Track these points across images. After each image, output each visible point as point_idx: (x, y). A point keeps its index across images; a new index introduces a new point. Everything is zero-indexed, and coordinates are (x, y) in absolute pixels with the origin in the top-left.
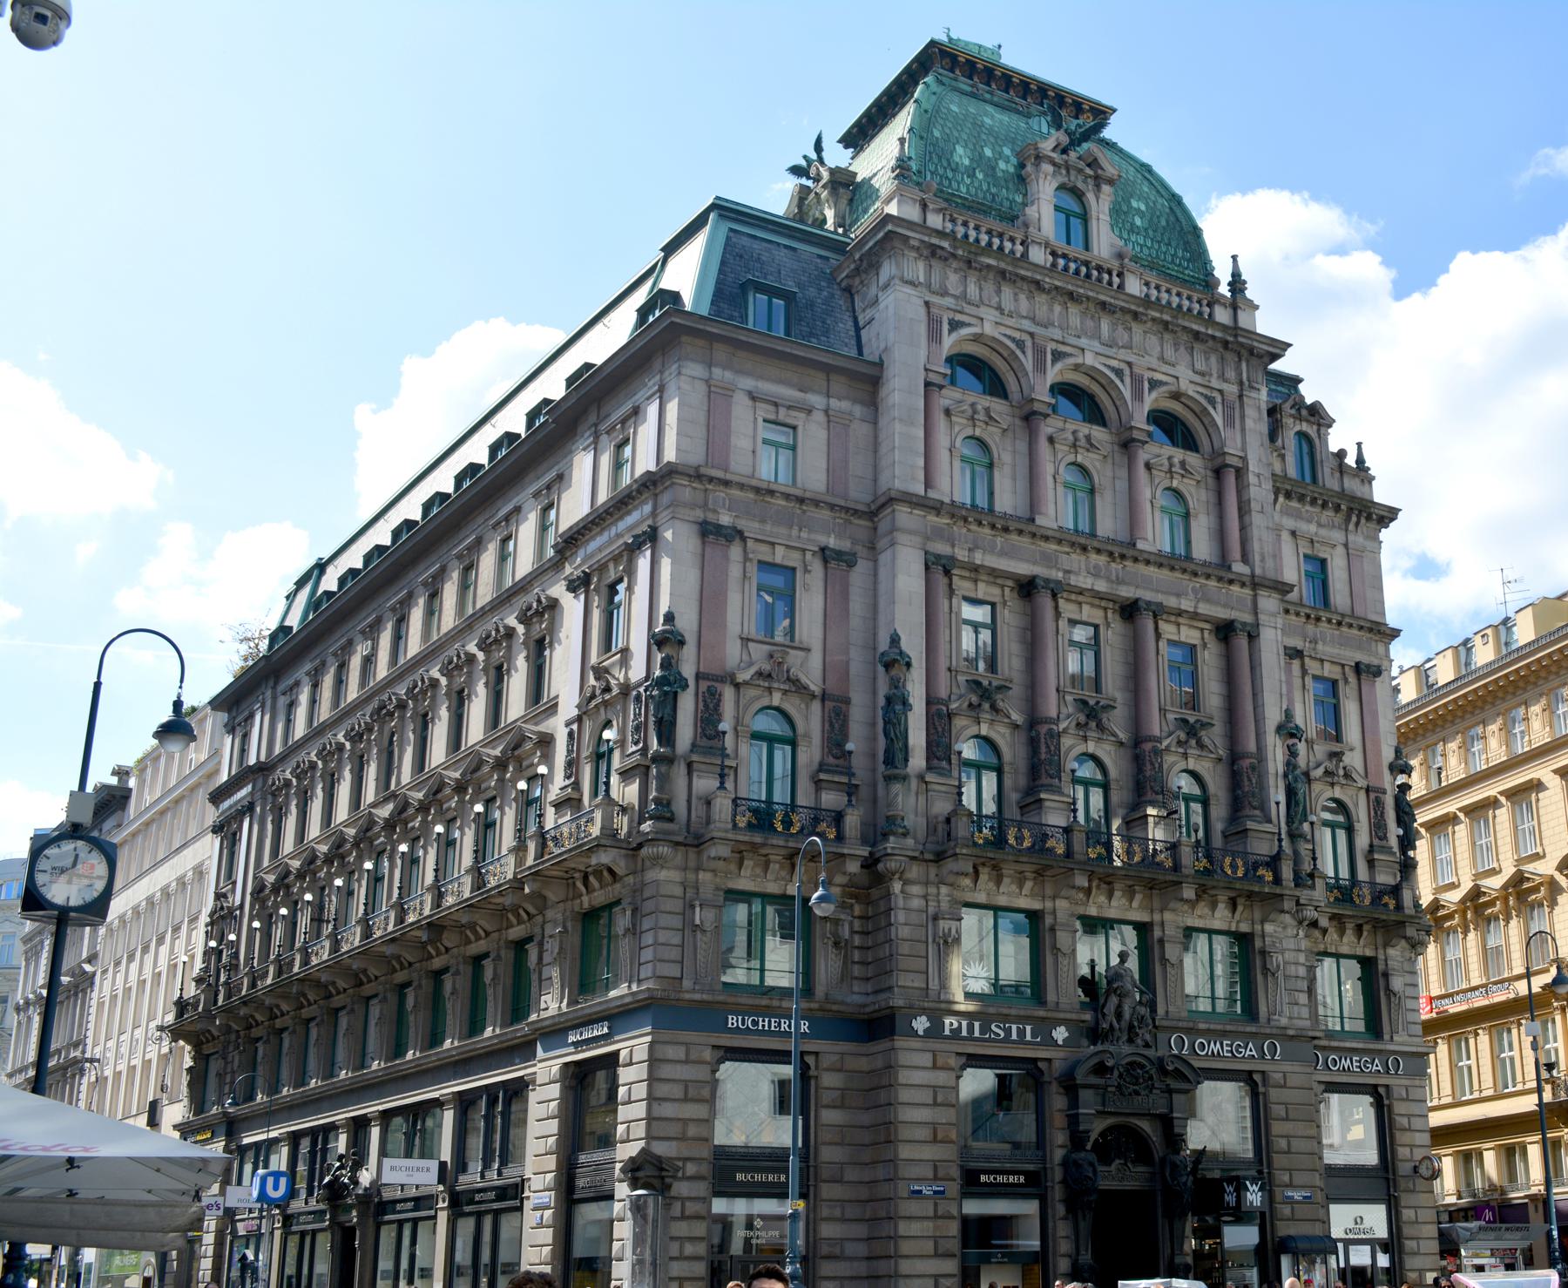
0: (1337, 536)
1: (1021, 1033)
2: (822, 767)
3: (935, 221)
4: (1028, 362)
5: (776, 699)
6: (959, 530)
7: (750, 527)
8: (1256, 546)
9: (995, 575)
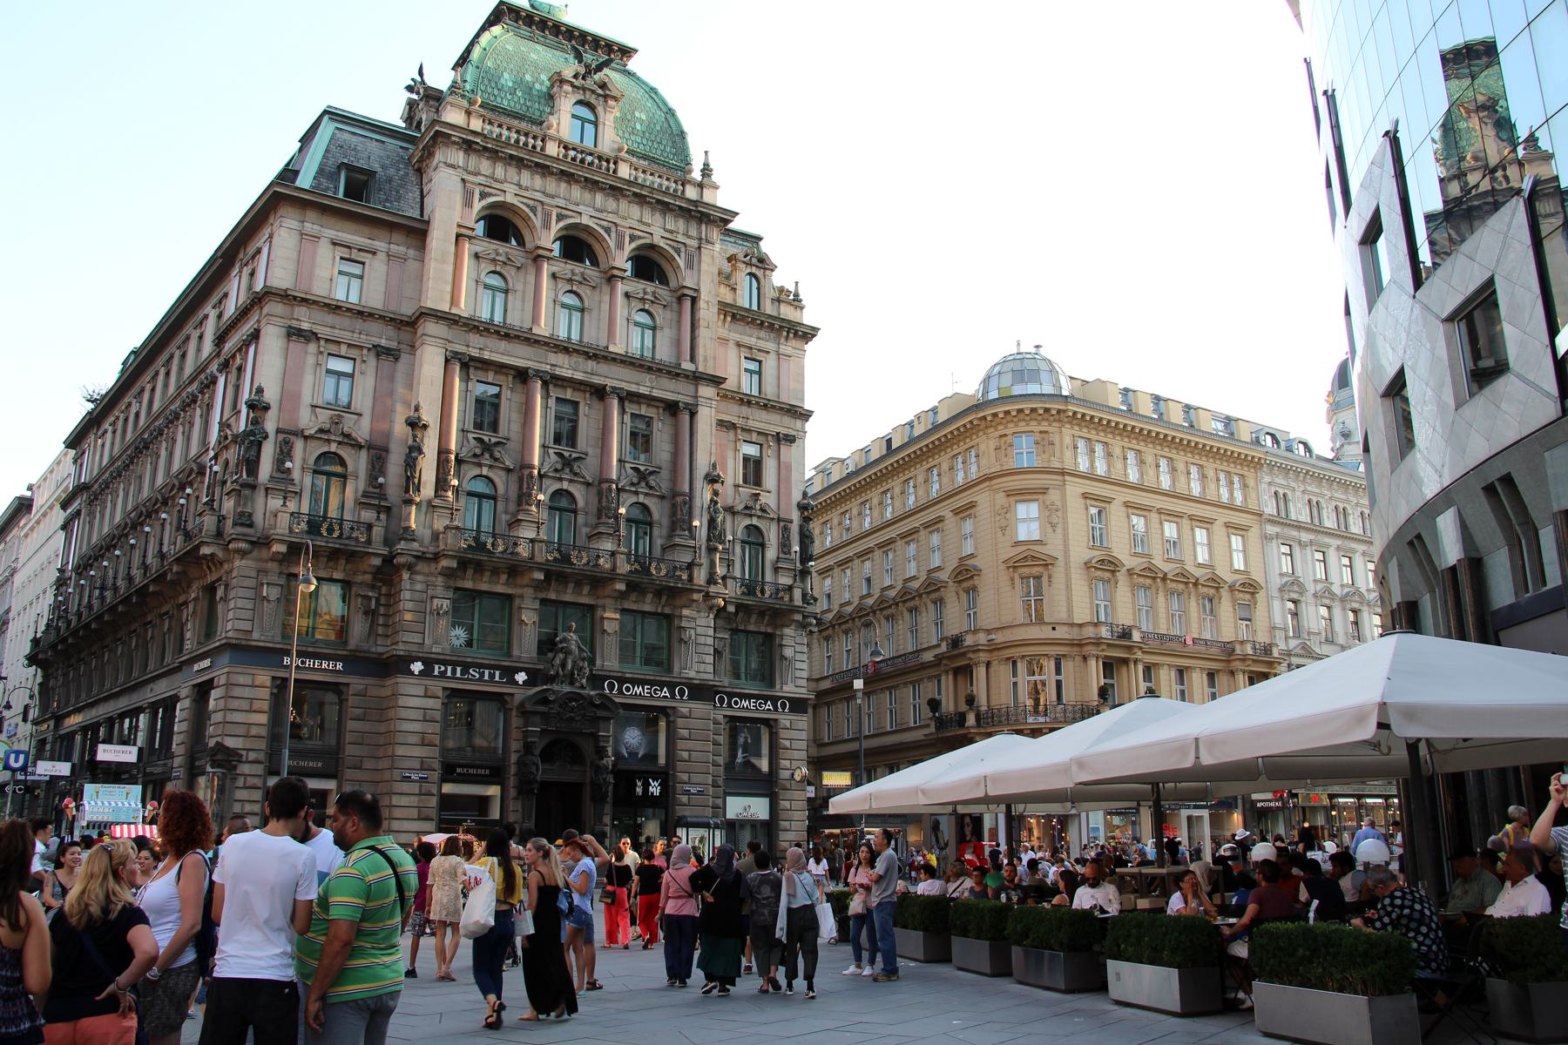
0: (771, 346)
1: (492, 676)
2: (365, 494)
3: (476, 124)
4: (537, 221)
5: (333, 447)
7: (322, 331)
8: (701, 352)
9: (501, 368)
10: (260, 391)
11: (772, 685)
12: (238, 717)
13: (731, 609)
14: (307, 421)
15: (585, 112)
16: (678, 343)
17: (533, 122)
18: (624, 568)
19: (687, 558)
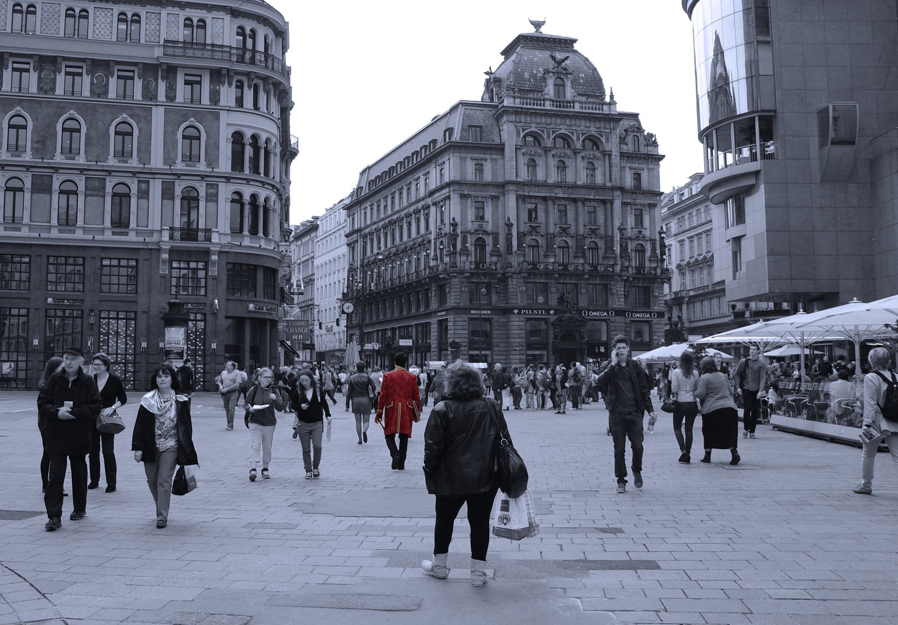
0: (644, 166)
4: (545, 136)
6: (526, 188)
8: (613, 177)
10: (454, 219)
11: (649, 307)
12: (458, 332)
13: (631, 279)
14: (470, 227)
15: (560, 82)
16: (605, 174)
17: (539, 92)
18: (588, 268)
19: (612, 263)
